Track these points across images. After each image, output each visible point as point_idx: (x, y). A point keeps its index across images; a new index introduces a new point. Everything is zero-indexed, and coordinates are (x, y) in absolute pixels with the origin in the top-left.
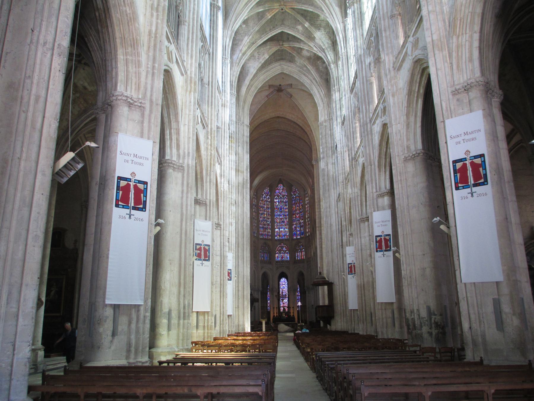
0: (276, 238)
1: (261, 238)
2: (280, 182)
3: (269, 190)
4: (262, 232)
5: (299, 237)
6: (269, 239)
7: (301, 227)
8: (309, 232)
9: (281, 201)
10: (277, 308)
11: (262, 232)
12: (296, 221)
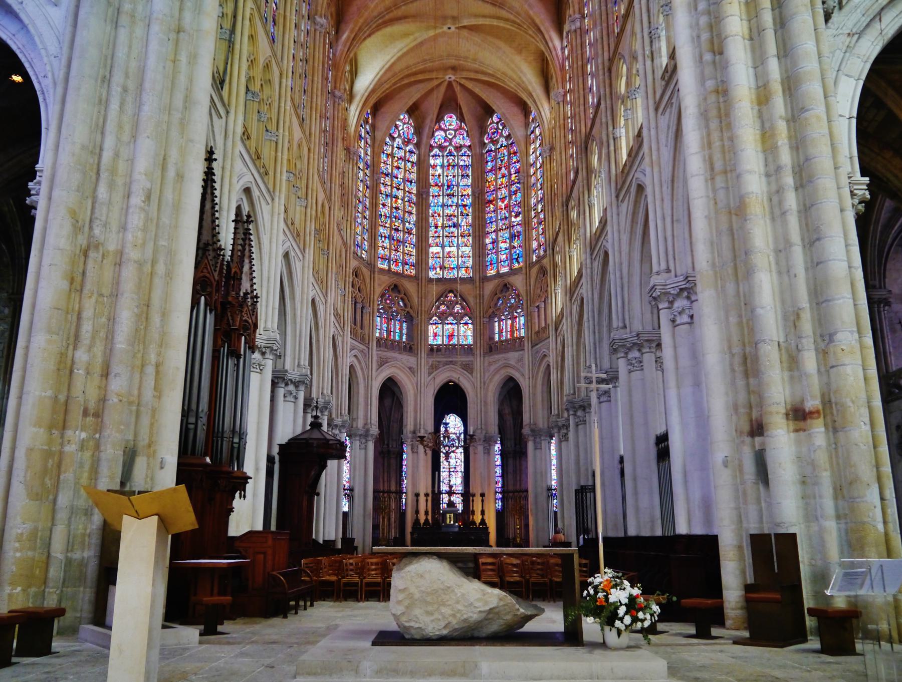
0: (432, 274)
1: (382, 270)
2: (449, 104)
3: (415, 128)
4: (387, 252)
6: (409, 277)
7: (512, 237)
8: (540, 246)
10: (427, 495)
11: (387, 252)
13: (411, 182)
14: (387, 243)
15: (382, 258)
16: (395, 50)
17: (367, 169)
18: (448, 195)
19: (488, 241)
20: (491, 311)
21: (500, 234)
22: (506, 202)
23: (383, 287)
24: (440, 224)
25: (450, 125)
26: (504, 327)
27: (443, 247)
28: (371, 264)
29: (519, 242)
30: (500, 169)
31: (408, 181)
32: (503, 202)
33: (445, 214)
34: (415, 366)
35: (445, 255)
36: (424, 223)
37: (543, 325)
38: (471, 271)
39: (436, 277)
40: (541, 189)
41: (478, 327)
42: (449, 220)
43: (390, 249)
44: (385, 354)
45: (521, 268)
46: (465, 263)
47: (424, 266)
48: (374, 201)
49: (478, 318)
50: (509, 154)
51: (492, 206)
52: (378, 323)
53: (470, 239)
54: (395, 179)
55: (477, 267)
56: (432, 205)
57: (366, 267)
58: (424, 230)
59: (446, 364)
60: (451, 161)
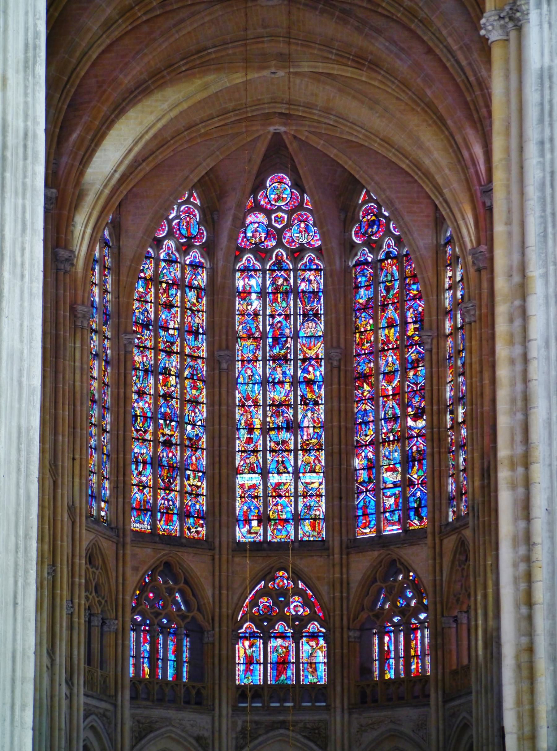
1: (139, 534)
3: (202, 210)
5: (393, 530)
6: (195, 543)
8: (461, 494)
9: (276, 291)
12: (376, 422)
13: (196, 333)
14: (147, 476)
15: (138, 509)
16: (165, 106)
17: (106, 324)
18: (275, 358)
19: (358, 463)
20: (364, 615)
21: (384, 451)
22: (395, 383)
23: (141, 573)
24: (257, 423)
25: (279, 199)
26: (392, 648)
27: (265, 474)
28: (117, 528)
29: (421, 473)
30: (384, 307)
31: (190, 332)
32: (390, 382)
33: (269, 402)
34: (207, 734)
35: (269, 491)
36: (224, 426)
37: (465, 661)
38: (323, 525)
39: (250, 538)
40: (463, 374)
41: (338, 651)
42: (277, 414)
43: (155, 488)
44: (146, 712)
45: (424, 530)
46: (309, 508)
47: (224, 518)
48: (122, 391)
49: (338, 631)
50: (403, 278)
51: (366, 387)
52: (132, 644)
53: (322, 456)
54: (162, 333)
55: (337, 521)
56: (241, 380)
57: (108, 538)
58: (224, 441)
59: (272, 727)
60: (280, 281)
